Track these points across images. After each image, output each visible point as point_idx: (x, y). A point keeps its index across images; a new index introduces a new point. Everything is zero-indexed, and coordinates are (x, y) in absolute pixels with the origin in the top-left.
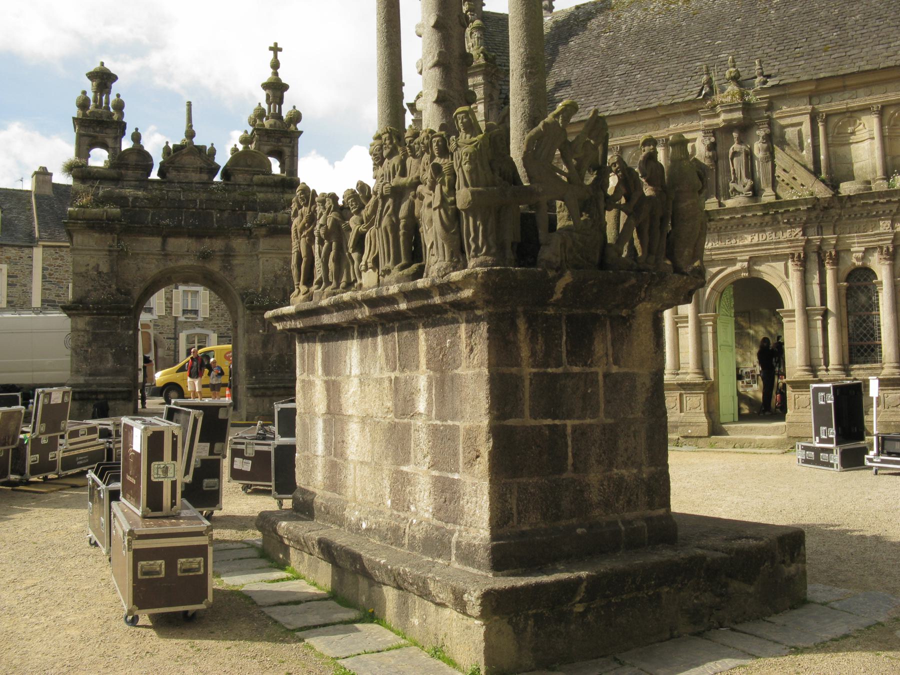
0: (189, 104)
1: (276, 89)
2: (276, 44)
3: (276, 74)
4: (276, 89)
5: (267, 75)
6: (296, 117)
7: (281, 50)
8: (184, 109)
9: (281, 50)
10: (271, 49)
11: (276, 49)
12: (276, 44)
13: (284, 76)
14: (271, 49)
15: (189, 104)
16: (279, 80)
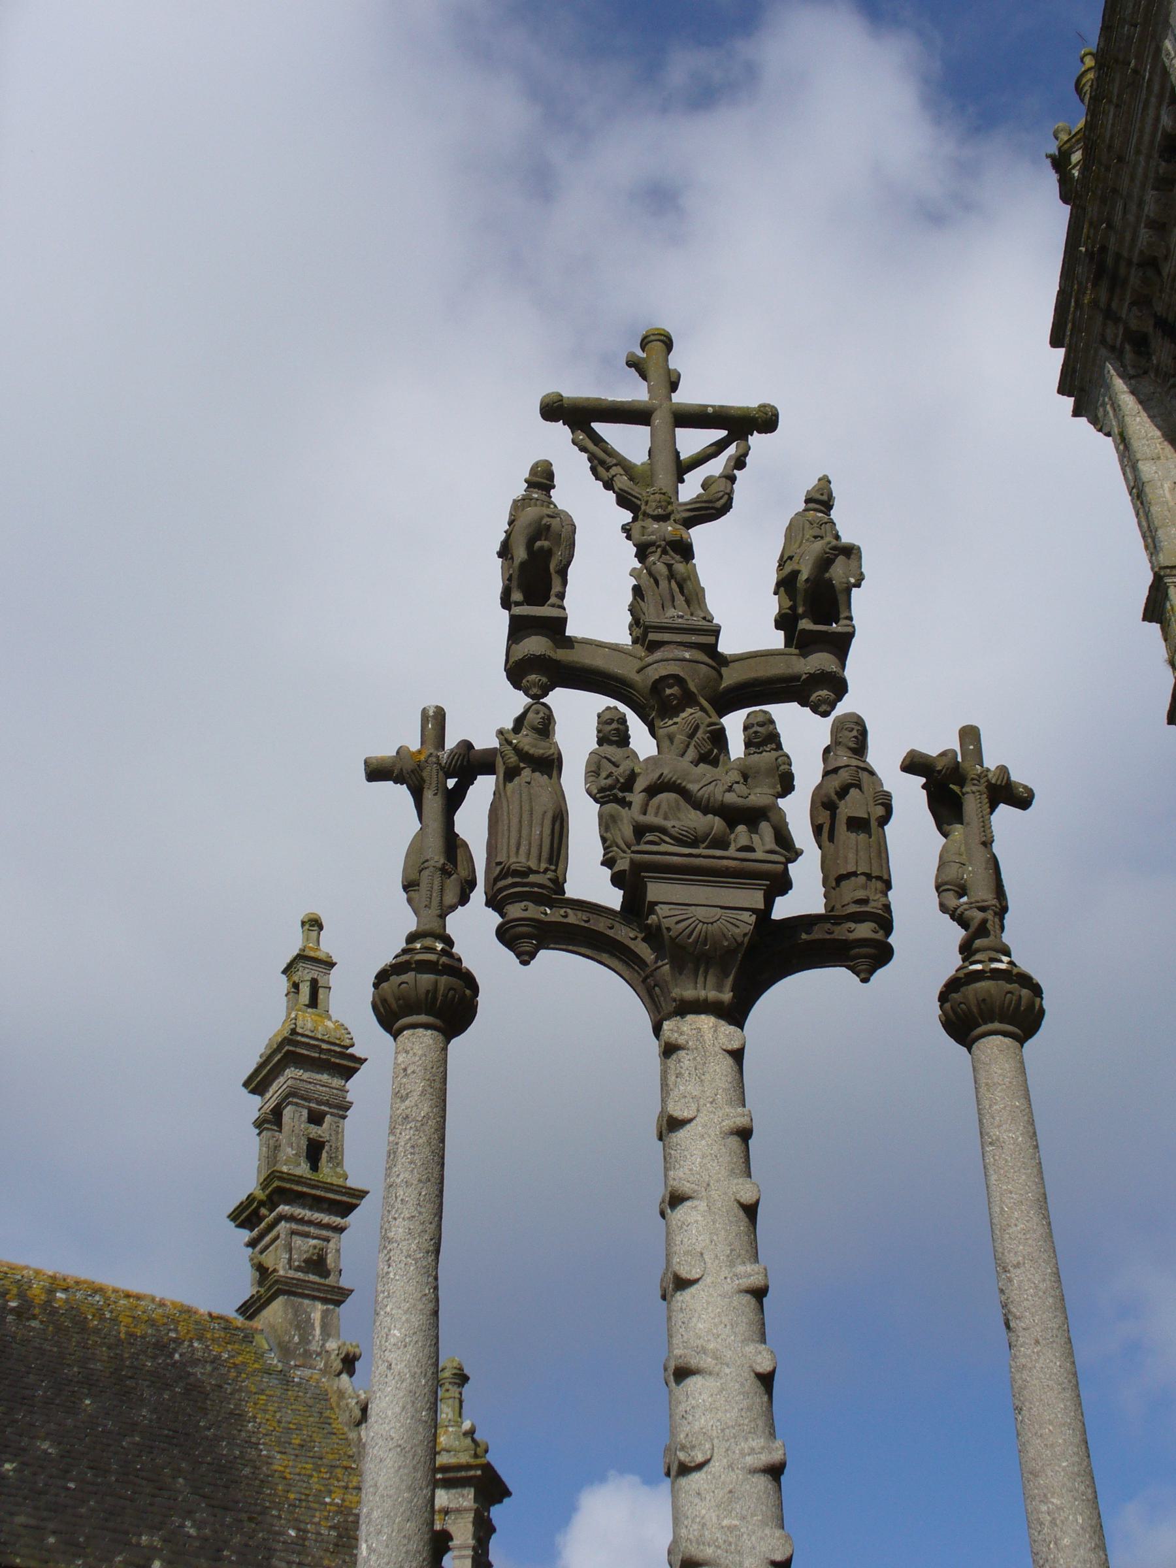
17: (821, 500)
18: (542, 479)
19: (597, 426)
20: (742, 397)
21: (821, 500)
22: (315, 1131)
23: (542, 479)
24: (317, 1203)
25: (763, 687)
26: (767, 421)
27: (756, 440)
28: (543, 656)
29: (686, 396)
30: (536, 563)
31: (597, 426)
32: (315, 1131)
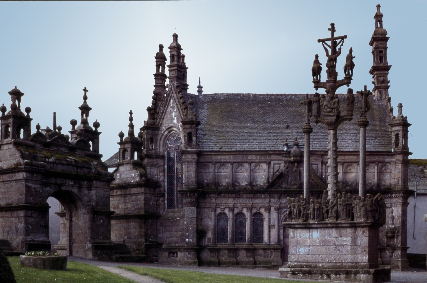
0: (55, 113)
1: (85, 109)
2: (85, 88)
3: (85, 102)
4: (85, 109)
5: (81, 102)
6: (97, 125)
7: (88, 91)
8: (53, 115)
9: (88, 91)
10: (84, 90)
11: (85, 90)
12: (85, 88)
13: (89, 103)
14: (84, 90)
15: (55, 113)
16: (87, 106)
17: (351, 51)
18: (317, 56)
19: (326, 42)
20: (342, 35)
21: (351, 51)
22: (381, 55)
23: (317, 56)
24: (382, 70)
25: (342, 83)
26: (346, 37)
27: (345, 39)
28: (317, 84)
29: (336, 35)
30: (316, 71)
31: (326, 42)
32: (381, 55)
